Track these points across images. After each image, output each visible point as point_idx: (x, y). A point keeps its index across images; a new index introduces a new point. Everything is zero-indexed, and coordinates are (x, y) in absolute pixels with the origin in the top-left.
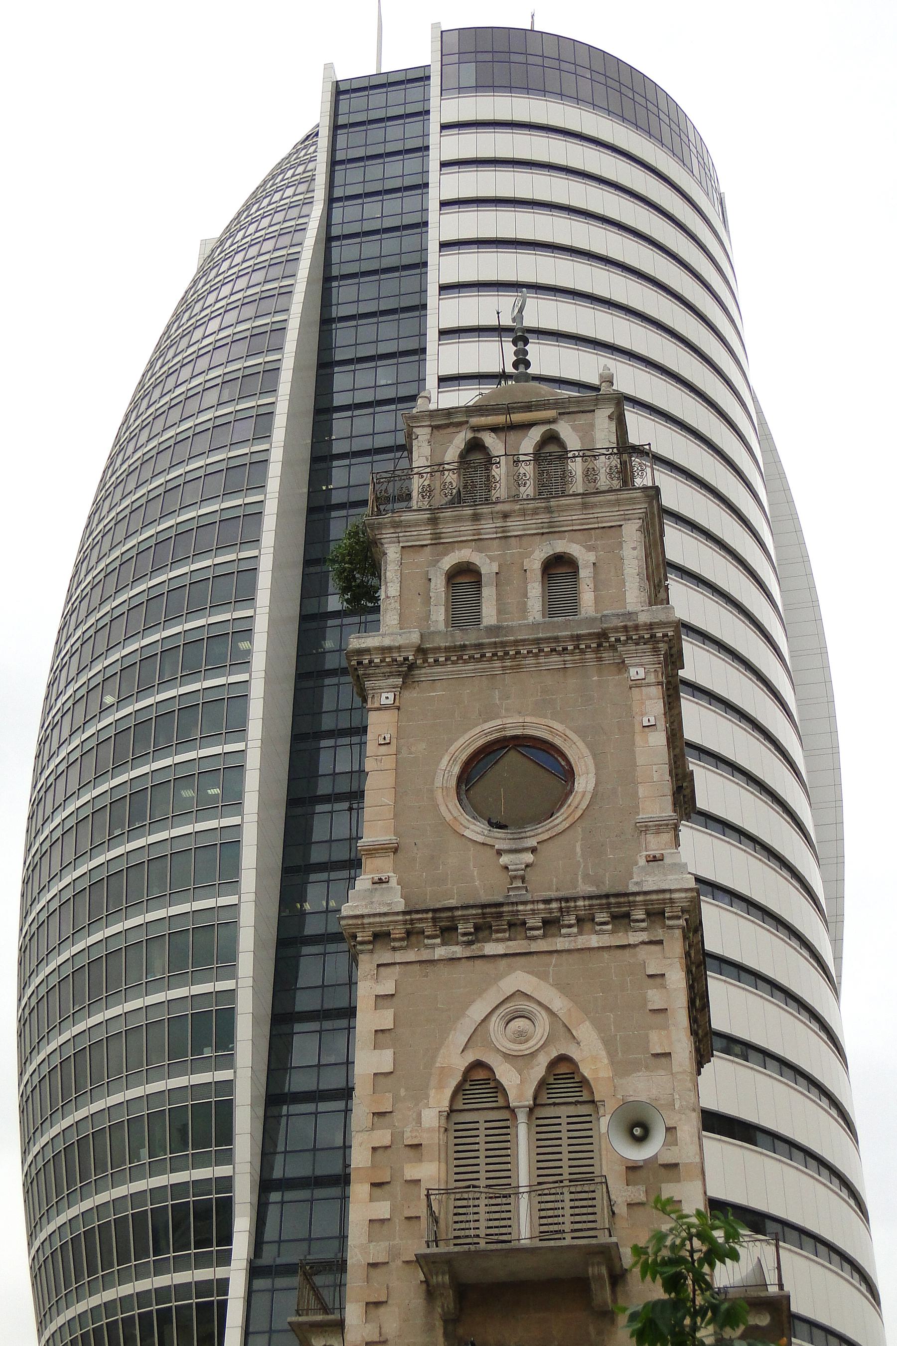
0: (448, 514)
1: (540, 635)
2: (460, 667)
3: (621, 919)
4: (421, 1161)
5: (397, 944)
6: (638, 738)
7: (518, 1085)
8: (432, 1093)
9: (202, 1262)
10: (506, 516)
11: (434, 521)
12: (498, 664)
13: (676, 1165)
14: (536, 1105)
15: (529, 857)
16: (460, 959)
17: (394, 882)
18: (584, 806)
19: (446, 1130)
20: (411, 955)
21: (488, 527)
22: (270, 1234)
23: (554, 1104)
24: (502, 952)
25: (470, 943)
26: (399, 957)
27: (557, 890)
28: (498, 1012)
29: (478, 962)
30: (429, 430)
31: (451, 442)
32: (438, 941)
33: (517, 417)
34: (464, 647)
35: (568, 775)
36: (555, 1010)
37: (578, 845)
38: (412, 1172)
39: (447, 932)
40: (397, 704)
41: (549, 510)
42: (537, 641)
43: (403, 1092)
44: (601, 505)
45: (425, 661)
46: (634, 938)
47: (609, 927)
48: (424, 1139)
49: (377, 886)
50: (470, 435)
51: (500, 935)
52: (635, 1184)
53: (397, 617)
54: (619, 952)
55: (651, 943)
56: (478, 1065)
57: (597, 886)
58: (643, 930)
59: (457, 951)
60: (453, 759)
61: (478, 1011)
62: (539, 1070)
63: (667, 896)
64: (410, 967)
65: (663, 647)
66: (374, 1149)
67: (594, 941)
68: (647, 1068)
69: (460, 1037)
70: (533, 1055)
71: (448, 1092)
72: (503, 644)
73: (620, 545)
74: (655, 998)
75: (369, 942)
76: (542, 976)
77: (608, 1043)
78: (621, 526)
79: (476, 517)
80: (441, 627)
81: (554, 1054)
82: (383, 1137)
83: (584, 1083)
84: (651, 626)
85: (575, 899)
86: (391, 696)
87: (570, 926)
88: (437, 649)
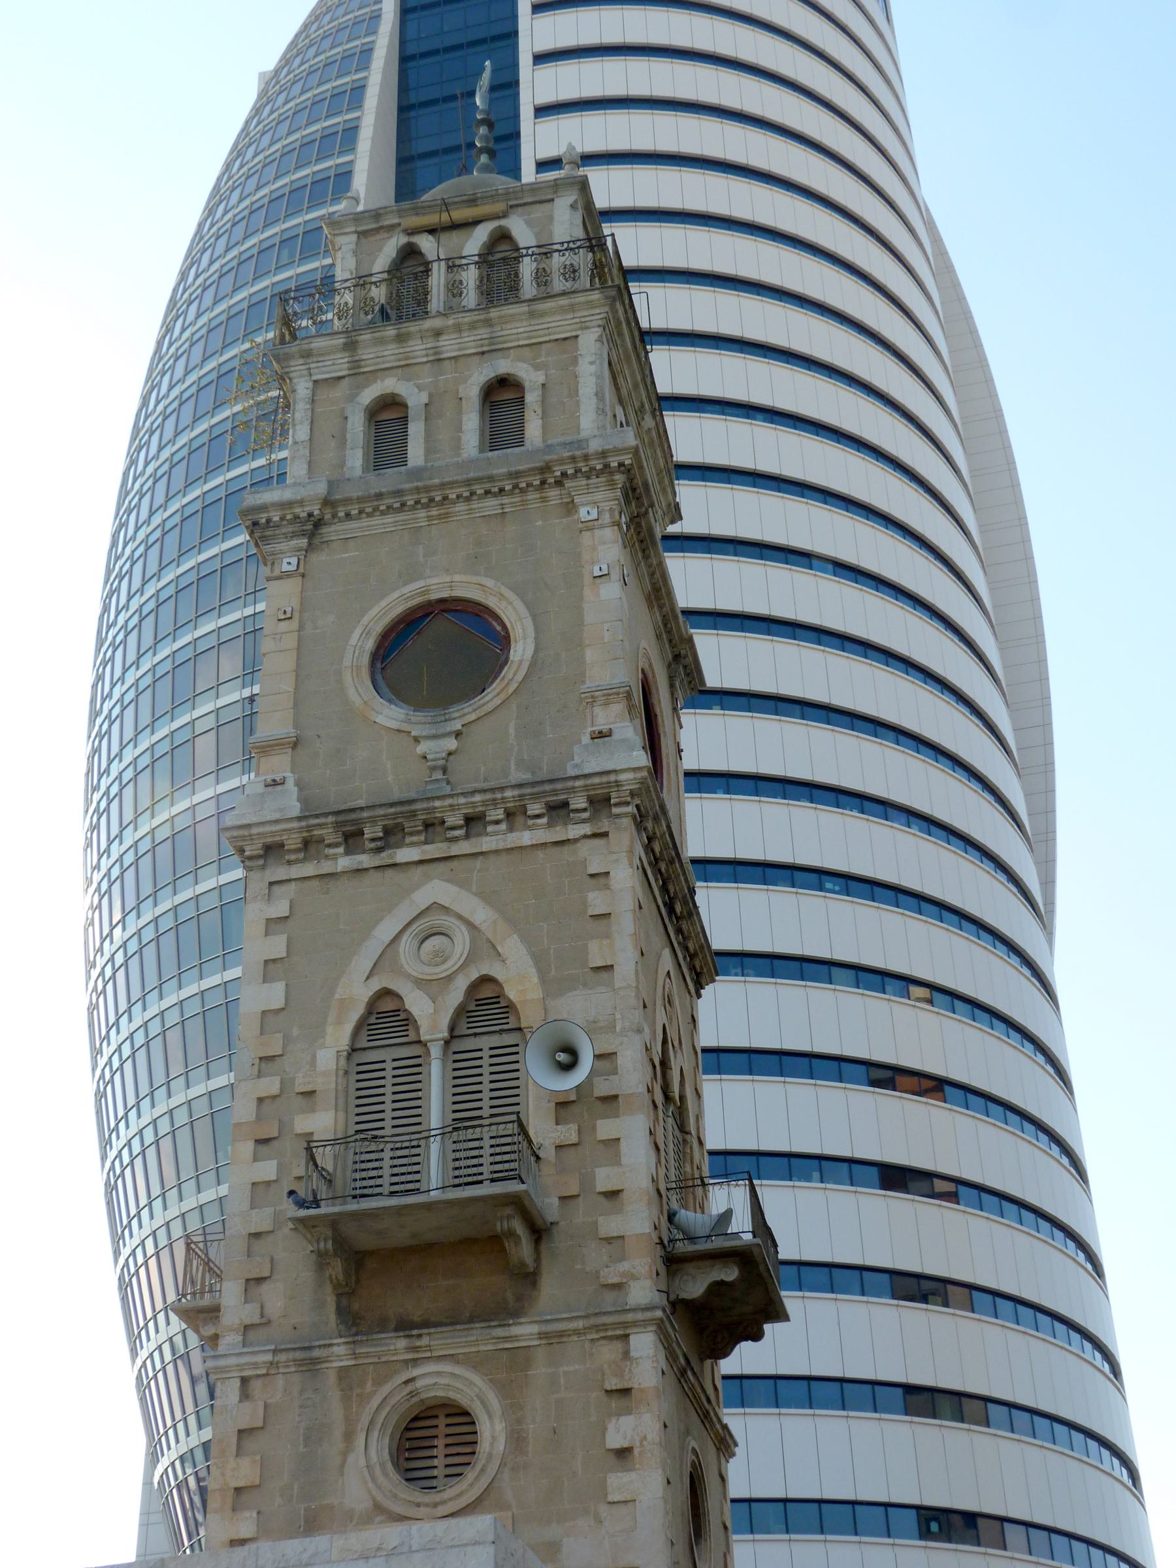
0: (366, 337)
1: (472, 475)
2: (377, 520)
3: (559, 810)
4: (313, 1111)
5: (293, 857)
6: (587, 592)
7: (431, 1015)
8: (329, 1030)
10: (438, 333)
11: (351, 346)
12: (422, 514)
13: (616, 1097)
14: (452, 1037)
15: (451, 744)
16: (366, 869)
17: (290, 783)
18: (520, 677)
19: (346, 1073)
20: (309, 869)
21: (418, 348)
23: (475, 1035)
24: (416, 858)
25: (379, 850)
26: (296, 871)
27: (486, 780)
28: (410, 930)
29: (389, 873)
30: (354, 237)
31: (380, 250)
32: (341, 850)
33: (459, 214)
34: (379, 496)
35: (504, 641)
36: (477, 923)
37: (512, 725)
38: (306, 1123)
39: (352, 838)
40: (301, 570)
41: (488, 323)
42: (468, 482)
43: (295, 1032)
44: (551, 312)
45: (334, 516)
46: (574, 831)
47: (544, 820)
48: (318, 1084)
49: (270, 789)
50: (404, 240)
51: (415, 839)
52: (566, 1122)
53: (306, 466)
54: (554, 851)
55: (595, 835)
56: (386, 993)
57: (533, 773)
58: (584, 821)
59: (365, 860)
60: (366, 633)
61: (386, 930)
62: (456, 995)
63: (612, 778)
64: (307, 884)
65: (620, 478)
66: (260, 1100)
67: (526, 838)
68: (585, 985)
69: (364, 962)
70: (450, 978)
71: (349, 1028)
72: (427, 489)
73: (575, 361)
74: (597, 902)
75: (259, 857)
76: (464, 884)
77: (540, 960)
78: (577, 337)
79: (401, 338)
80: (358, 472)
81: (474, 975)
82: (270, 1085)
83: (510, 1008)
84: (603, 454)
85: (502, 789)
86: (294, 561)
87: (497, 822)
88: (347, 501)
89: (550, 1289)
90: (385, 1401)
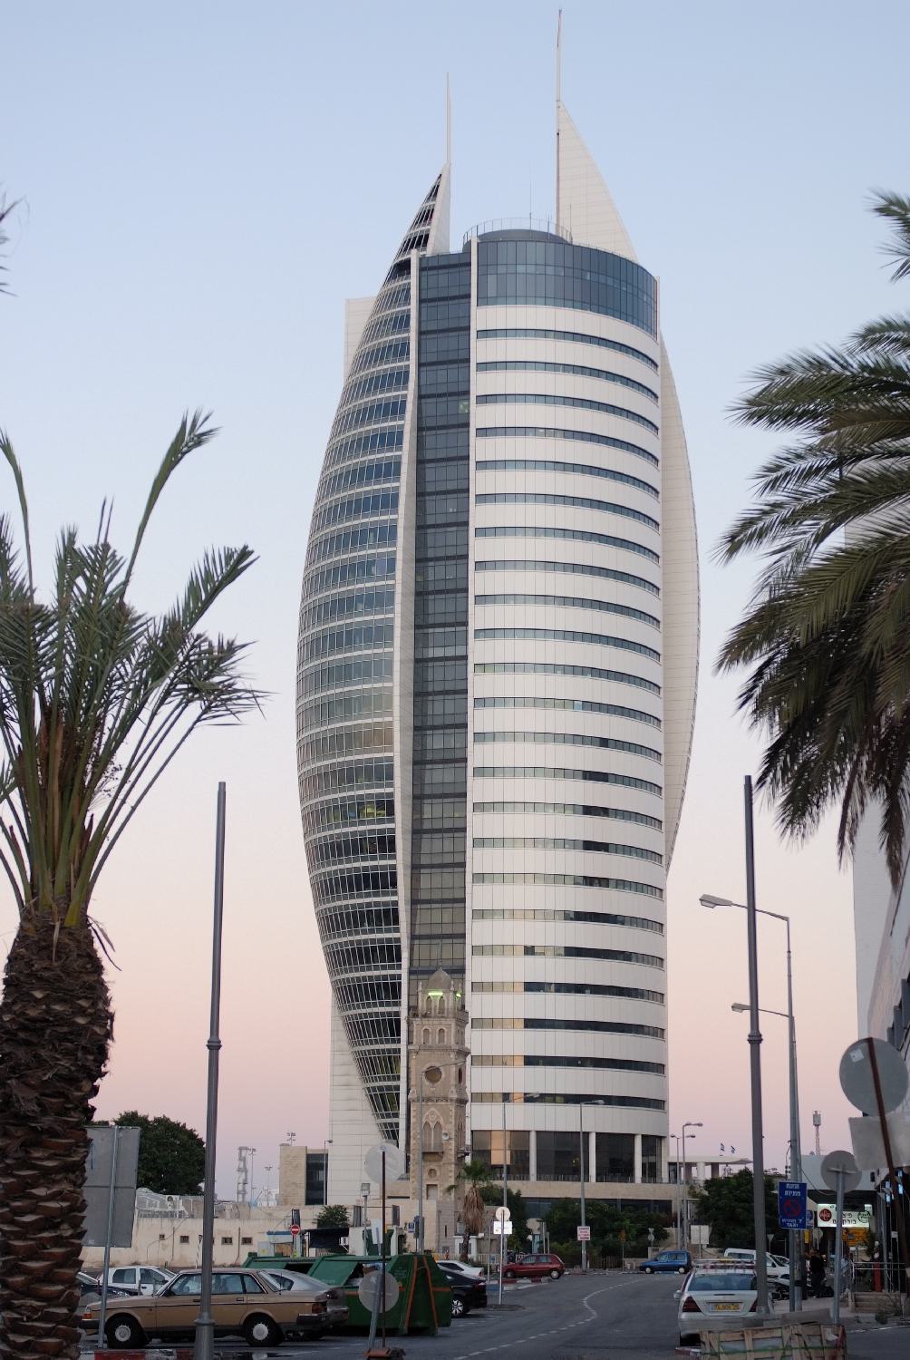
7: (432, 1125)
9: (392, 967)
21: (430, 1022)
22: (416, 956)
89: (444, 1159)
90: (427, 1169)
